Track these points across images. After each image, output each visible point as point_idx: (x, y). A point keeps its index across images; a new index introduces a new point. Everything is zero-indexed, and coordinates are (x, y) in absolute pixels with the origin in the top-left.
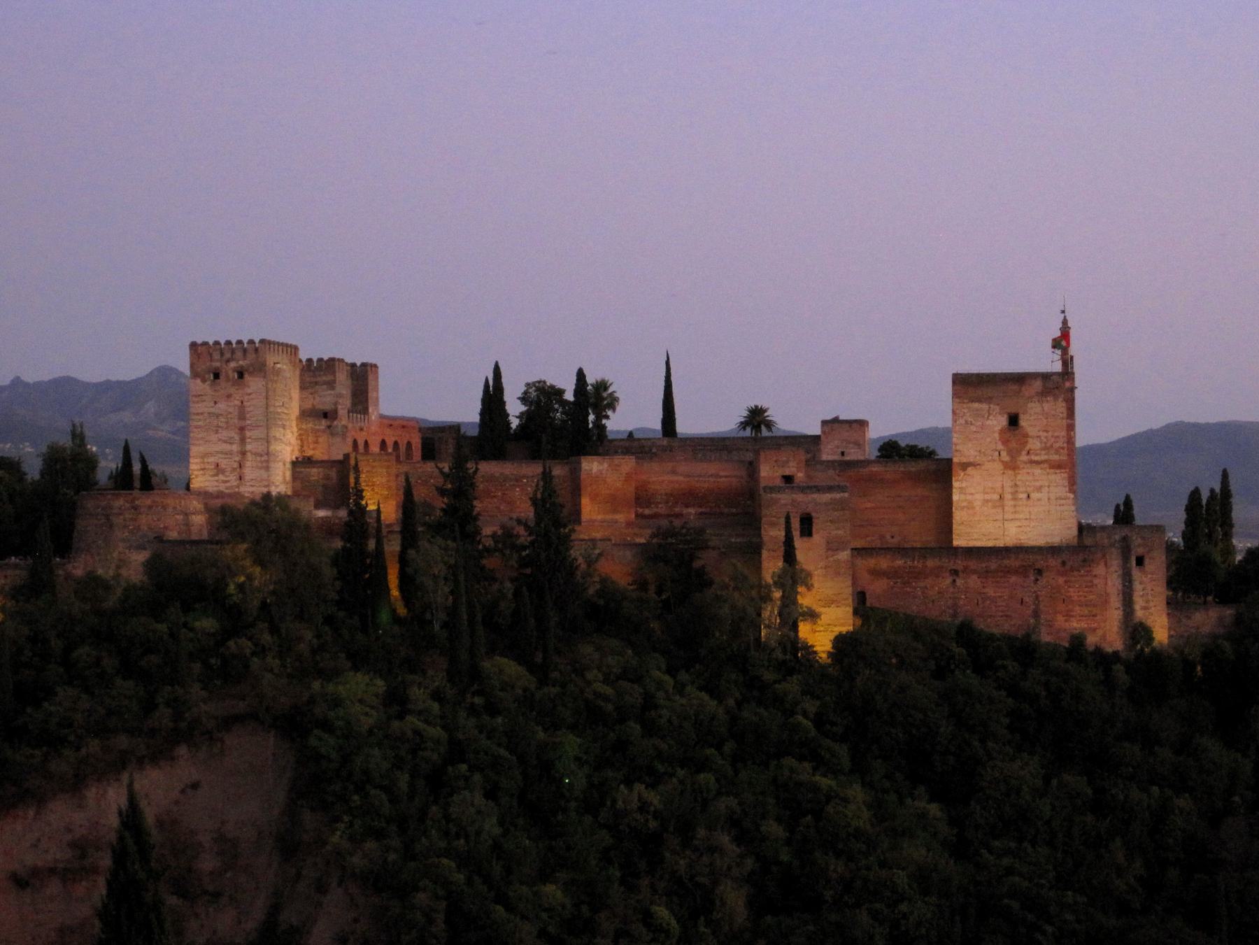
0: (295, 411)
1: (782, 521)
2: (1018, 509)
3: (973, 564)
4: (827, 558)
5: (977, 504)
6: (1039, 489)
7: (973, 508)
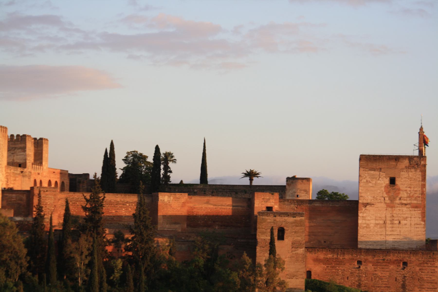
0: (5, 162)
1: (269, 230)
2: (394, 229)
3: (370, 258)
4: (292, 252)
5: (372, 225)
6: (405, 219)
7: (369, 227)
